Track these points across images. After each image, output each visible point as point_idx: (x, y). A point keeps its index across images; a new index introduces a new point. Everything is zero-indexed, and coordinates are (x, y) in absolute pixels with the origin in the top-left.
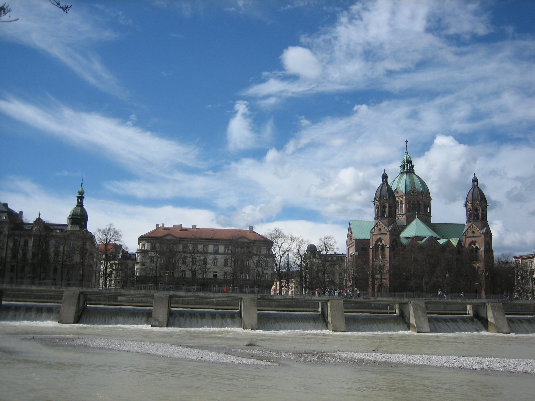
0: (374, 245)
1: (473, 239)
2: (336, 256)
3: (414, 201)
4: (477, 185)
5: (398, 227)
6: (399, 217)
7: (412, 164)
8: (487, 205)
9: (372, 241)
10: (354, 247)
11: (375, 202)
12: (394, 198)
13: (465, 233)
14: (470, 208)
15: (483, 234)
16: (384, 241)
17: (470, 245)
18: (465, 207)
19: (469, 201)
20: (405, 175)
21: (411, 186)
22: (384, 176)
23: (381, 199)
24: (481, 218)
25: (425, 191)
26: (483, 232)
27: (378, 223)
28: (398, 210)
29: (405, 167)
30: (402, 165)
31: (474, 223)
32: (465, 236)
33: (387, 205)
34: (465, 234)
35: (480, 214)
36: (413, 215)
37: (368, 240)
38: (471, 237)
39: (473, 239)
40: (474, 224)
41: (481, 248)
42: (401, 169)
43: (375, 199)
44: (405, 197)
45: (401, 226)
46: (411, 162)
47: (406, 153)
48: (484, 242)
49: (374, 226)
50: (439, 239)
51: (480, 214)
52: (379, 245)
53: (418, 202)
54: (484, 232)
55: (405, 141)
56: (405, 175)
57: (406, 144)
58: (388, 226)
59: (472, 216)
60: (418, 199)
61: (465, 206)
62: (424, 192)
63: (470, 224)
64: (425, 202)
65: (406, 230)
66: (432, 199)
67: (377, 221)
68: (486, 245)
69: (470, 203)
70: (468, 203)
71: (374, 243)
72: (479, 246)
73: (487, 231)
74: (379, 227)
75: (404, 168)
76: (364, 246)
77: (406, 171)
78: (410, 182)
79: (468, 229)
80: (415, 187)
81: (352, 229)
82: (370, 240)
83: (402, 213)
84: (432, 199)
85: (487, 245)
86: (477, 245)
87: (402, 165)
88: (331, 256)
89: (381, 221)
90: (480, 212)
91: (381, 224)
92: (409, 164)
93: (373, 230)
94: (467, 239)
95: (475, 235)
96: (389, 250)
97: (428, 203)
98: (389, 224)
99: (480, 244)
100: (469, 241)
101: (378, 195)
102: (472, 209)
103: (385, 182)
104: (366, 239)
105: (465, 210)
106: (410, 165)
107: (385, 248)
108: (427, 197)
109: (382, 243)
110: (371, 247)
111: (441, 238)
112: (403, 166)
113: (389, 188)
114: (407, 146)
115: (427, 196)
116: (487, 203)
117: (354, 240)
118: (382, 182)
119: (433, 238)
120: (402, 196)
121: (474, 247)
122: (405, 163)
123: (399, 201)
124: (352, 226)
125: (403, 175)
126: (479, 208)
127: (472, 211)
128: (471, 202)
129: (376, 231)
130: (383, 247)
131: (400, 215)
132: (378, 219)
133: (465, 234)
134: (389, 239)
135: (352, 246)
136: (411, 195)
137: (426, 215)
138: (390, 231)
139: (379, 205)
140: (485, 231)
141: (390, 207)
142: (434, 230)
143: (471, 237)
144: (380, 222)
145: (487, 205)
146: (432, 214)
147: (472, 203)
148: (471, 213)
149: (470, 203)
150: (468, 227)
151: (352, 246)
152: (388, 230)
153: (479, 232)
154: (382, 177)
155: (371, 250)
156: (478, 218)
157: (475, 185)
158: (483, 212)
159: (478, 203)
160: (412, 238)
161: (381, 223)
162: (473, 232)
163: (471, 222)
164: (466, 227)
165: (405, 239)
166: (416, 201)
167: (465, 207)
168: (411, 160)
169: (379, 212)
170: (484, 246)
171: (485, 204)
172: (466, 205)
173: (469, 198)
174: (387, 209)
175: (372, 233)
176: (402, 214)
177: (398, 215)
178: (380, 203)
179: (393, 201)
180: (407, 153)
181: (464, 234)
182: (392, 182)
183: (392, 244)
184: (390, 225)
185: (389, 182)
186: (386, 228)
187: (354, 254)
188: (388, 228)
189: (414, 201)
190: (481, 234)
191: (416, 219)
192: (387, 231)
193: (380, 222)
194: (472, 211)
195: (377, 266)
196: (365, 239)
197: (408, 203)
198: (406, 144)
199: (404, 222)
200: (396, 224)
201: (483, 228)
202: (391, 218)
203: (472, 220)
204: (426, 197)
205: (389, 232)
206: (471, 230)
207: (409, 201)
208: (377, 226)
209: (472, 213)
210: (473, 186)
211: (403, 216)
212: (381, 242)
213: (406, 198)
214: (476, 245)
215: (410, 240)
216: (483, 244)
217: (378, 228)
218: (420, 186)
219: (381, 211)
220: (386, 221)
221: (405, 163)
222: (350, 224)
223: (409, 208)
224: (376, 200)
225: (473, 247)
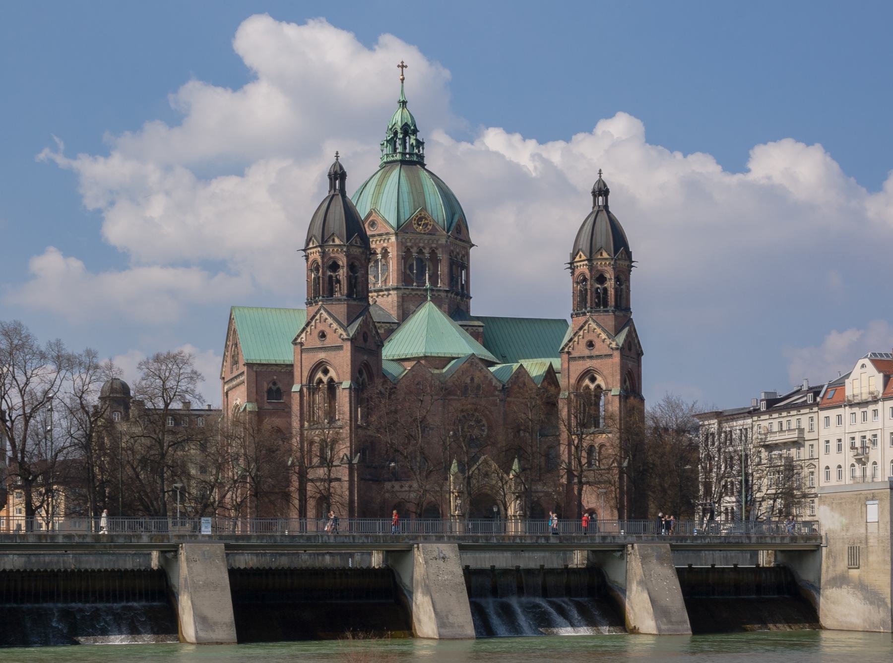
0: (304, 382)
1: (588, 364)
2: (188, 416)
3: (420, 252)
4: (606, 207)
5: (375, 327)
6: (377, 297)
7: (418, 138)
8: (633, 264)
9: (299, 369)
10: (243, 388)
11: (309, 251)
12: (365, 240)
13: (566, 345)
14: (583, 274)
15: (617, 349)
16: (335, 369)
17: (581, 379)
18: (570, 271)
19: (581, 253)
20: (398, 169)
21: (414, 205)
22: (336, 173)
23: (327, 241)
24: (613, 304)
25: (456, 220)
26: (617, 345)
27: (318, 317)
28: (376, 277)
29: (398, 146)
30: (387, 141)
31: (594, 317)
32: (567, 355)
33: (343, 261)
34: (566, 350)
35: (611, 292)
36: (419, 293)
37: (287, 365)
38: (582, 358)
39: (588, 364)
40: (592, 319)
41: (611, 390)
42: (385, 152)
43: (308, 244)
44: (397, 239)
45: (383, 325)
46: (415, 132)
47: (399, 102)
48: (619, 371)
49: (303, 325)
50: (492, 364)
51: (611, 292)
52: (320, 381)
53: (433, 252)
54: (620, 345)
55: (399, 66)
56: (396, 172)
57: (402, 75)
59: (589, 297)
60: (434, 245)
61: (569, 266)
62: (452, 223)
63: (582, 319)
64: (455, 253)
65: (397, 337)
66: (473, 245)
67: (315, 308)
68: (625, 382)
69: (583, 257)
70: (577, 259)
71: (306, 374)
72: (607, 383)
73: (630, 342)
74: (321, 327)
75: (395, 149)
76: (274, 384)
77: (398, 157)
78: (412, 192)
79: (575, 335)
80: (424, 209)
81: (238, 332)
82: (292, 365)
83: (386, 286)
84: (473, 245)
85: (628, 383)
86: (600, 381)
87: (387, 141)
88: (176, 416)
89: (326, 311)
90: (610, 284)
91: (326, 319)
92: (407, 138)
93: (303, 335)
94: (572, 363)
95: (595, 352)
96: (348, 395)
97: (464, 256)
98: (348, 322)
99: (610, 380)
100: (578, 368)
101: (317, 231)
102: (588, 276)
103: (337, 192)
104: (282, 363)
105: (570, 279)
106: (413, 141)
107: (337, 391)
108: (461, 240)
109: (329, 375)
110: (296, 388)
111: (498, 361)
112: (392, 142)
113: (350, 213)
114: (402, 82)
115: (460, 237)
116: (633, 260)
117: (244, 365)
118: (330, 192)
119: (477, 361)
120: (387, 234)
121: (592, 386)
122: (396, 133)
123: (379, 251)
124: (237, 325)
125: (392, 170)
126: (610, 274)
127: (589, 283)
128: (588, 254)
129: (310, 340)
130: (332, 386)
131: (381, 293)
132: (316, 302)
133: (566, 350)
134: (349, 362)
135: (238, 385)
136: (415, 232)
137: (457, 294)
138: (353, 340)
139: (320, 260)
140: (625, 340)
141: (352, 267)
142: (476, 335)
143: (582, 358)
144: (322, 311)
145: (633, 264)
146: (474, 290)
147: (590, 260)
148: (586, 290)
149: (583, 257)
150: (577, 329)
151: (238, 385)
152: (346, 337)
153: (608, 343)
154: (330, 175)
155: (298, 395)
156: (606, 304)
157: (599, 206)
158: (620, 285)
159: (606, 259)
160: (418, 359)
161: (325, 315)
162: (590, 344)
163: (584, 314)
164: (570, 329)
165: (395, 364)
166: (426, 252)
167: (570, 271)
168: (415, 126)
169: (319, 283)
170: (619, 385)
171: (627, 263)
172: (572, 265)
173: (581, 243)
174: (342, 273)
175: (299, 346)
176: (388, 290)
177: (375, 291)
178: (323, 254)
179: (361, 250)
180: (404, 103)
181: (563, 349)
182: (359, 189)
183: (358, 378)
184: (350, 322)
185: (352, 188)
186: (340, 331)
187: (245, 408)
188: (345, 330)
189: (421, 250)
190: (612, 348)
192: (343, 339)
193: (322, 311)
194: (589, 283)
195: (311, 443)
196: (277, 365)
197: (405, 256)
198: (402, 75)
199: (392, 312)
200: (369, 319)
201: (618, 332)
202: (355, 300)
203: (589, 309)
204: (456, 238)
205: (349, 343)
206: (583, 338)
207: (408, 251)
208: (313, 323)
209: (589, 287)
210: (593, 208)
211: (388, 296)
212: (326, 372)
213: (399, 240)
214: (597, 383)
215: (409, 366)
216: (618, 377)
217: (318, 331)
218: (439, 206)
219: (327, 279)
220: (341, 310)
221: (396, 133)
222: (231, 319)
223: (408, 272)
224: (311, 245)
225: (587, 387)
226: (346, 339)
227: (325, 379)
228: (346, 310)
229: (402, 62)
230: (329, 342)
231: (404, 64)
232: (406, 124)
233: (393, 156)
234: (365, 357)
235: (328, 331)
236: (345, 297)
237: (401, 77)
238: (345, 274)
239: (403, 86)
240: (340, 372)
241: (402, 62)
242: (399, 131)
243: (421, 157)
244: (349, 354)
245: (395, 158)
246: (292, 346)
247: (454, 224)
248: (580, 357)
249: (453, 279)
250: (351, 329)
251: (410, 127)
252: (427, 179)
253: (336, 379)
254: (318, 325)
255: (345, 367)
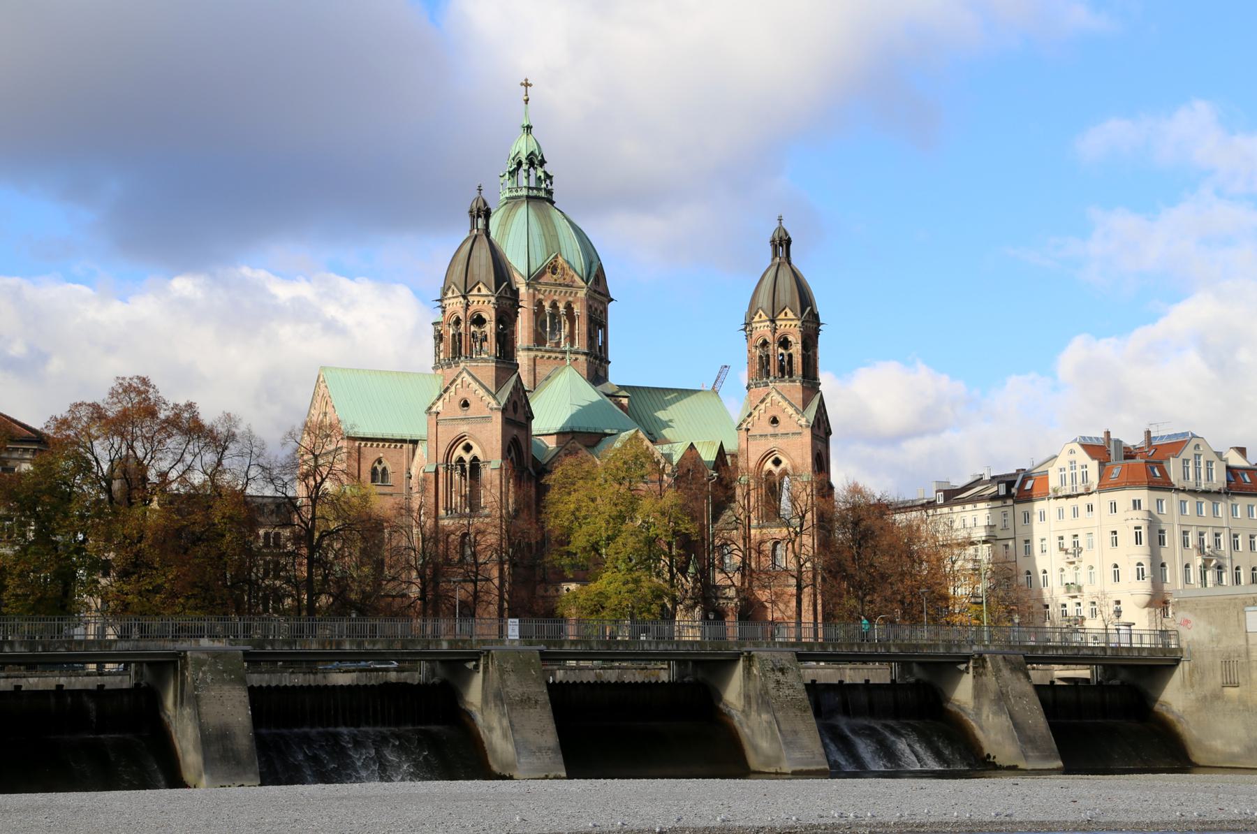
3: (554, 305)
24: (801, 373)
27: (459, 381)
46: (542, 163)
53: (569, 307)
55: (522, 84)
56: (523, 209)
58: (493, 391)
66: (612, 300)
74: (463, 394)
77: (524, 192)
78: (544, 235)
84: (612, 300)
90: (796, 349)
93: (440, 403)
102: (769, 339)
106: (540, 173)
108: (599, 293)
109: (472, 452)
114: (527, 103)
115: (599, 289)
125: (516, 206)
132: (457, 364)
144: (465, 374)
152: (495, 406)
161: (468, 379)
166: (561, 306)
168: (542, 156)
191: (567, 369)
192: (491, 409)
198: (527, 95)
205: (499, 414)
208: (453, 389)
212: (468, 448)
221: (520, 164)
223: (539, 329)
224: (450, 294)
226: (496, 409)
228: (494, 374)
229: (526, 80)
231: (529, 82)
232: (532, 153)
233: (517, 191)
234: (515, 432)
236: (493, 358)
237: (525, 98)
238: (494, 331)
239: (527, 108)
241: (526, 80)
242: (524, 161)
243: (550, 192)
244: (499, 427)
245: (520, 193)
246: (426, 416)
247: (593, 274)
249: (591, 338)
250: (502, 397)
251: (537, 158)
252: (561, 220)
254: (459, 392)
255: (494, 443)
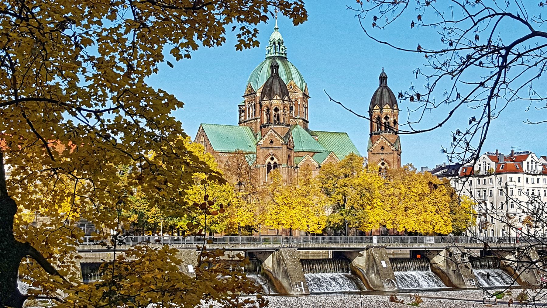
39: (381, 156)
52: (269, 163)
93: (262, 141)
109: (274, 160)
162: (382, 148)
208: (267, 136)
227: (272, 163)
230: (274, 145)
235: (274, 140)
240: (281, 159)
248: (377, 154)
253: (278, 163)
